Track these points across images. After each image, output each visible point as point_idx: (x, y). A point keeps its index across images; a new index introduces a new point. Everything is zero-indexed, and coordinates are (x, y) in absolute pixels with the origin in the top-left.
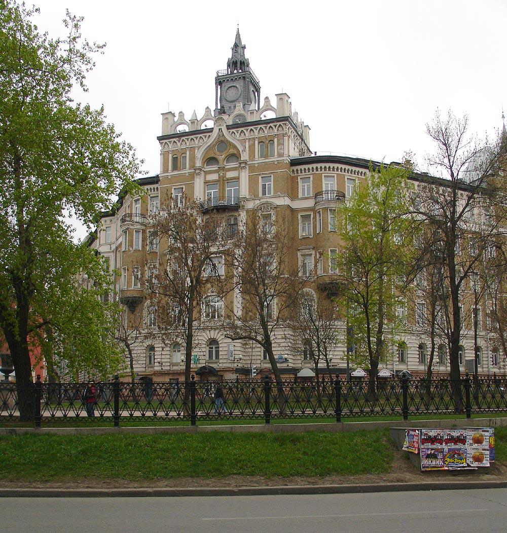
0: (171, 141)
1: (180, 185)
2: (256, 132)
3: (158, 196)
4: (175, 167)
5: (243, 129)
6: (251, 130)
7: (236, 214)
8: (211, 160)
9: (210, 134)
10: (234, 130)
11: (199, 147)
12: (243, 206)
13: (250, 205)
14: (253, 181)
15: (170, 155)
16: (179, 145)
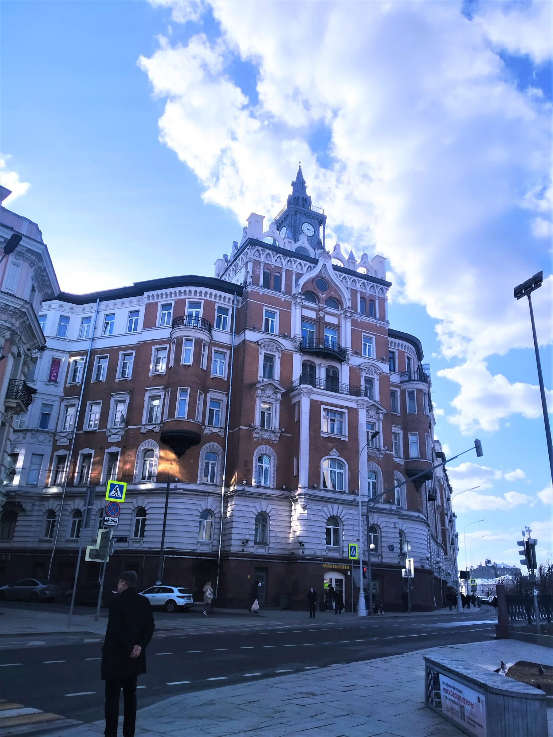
0: (265, 251)
1: (276, 309)
2: (359, 285)
3: (228, 310)
4: (266, 285)
5: (346, 275)
6: (354, 280)
7: (337, 365)
8: (309, 295)
9: (312, 265)
10: (337, 273)
11: (299, 276)
12: (348, 360)
13: (355, 361)
14: (355, 336)
15: (262, 267)
16: (274, 260)
